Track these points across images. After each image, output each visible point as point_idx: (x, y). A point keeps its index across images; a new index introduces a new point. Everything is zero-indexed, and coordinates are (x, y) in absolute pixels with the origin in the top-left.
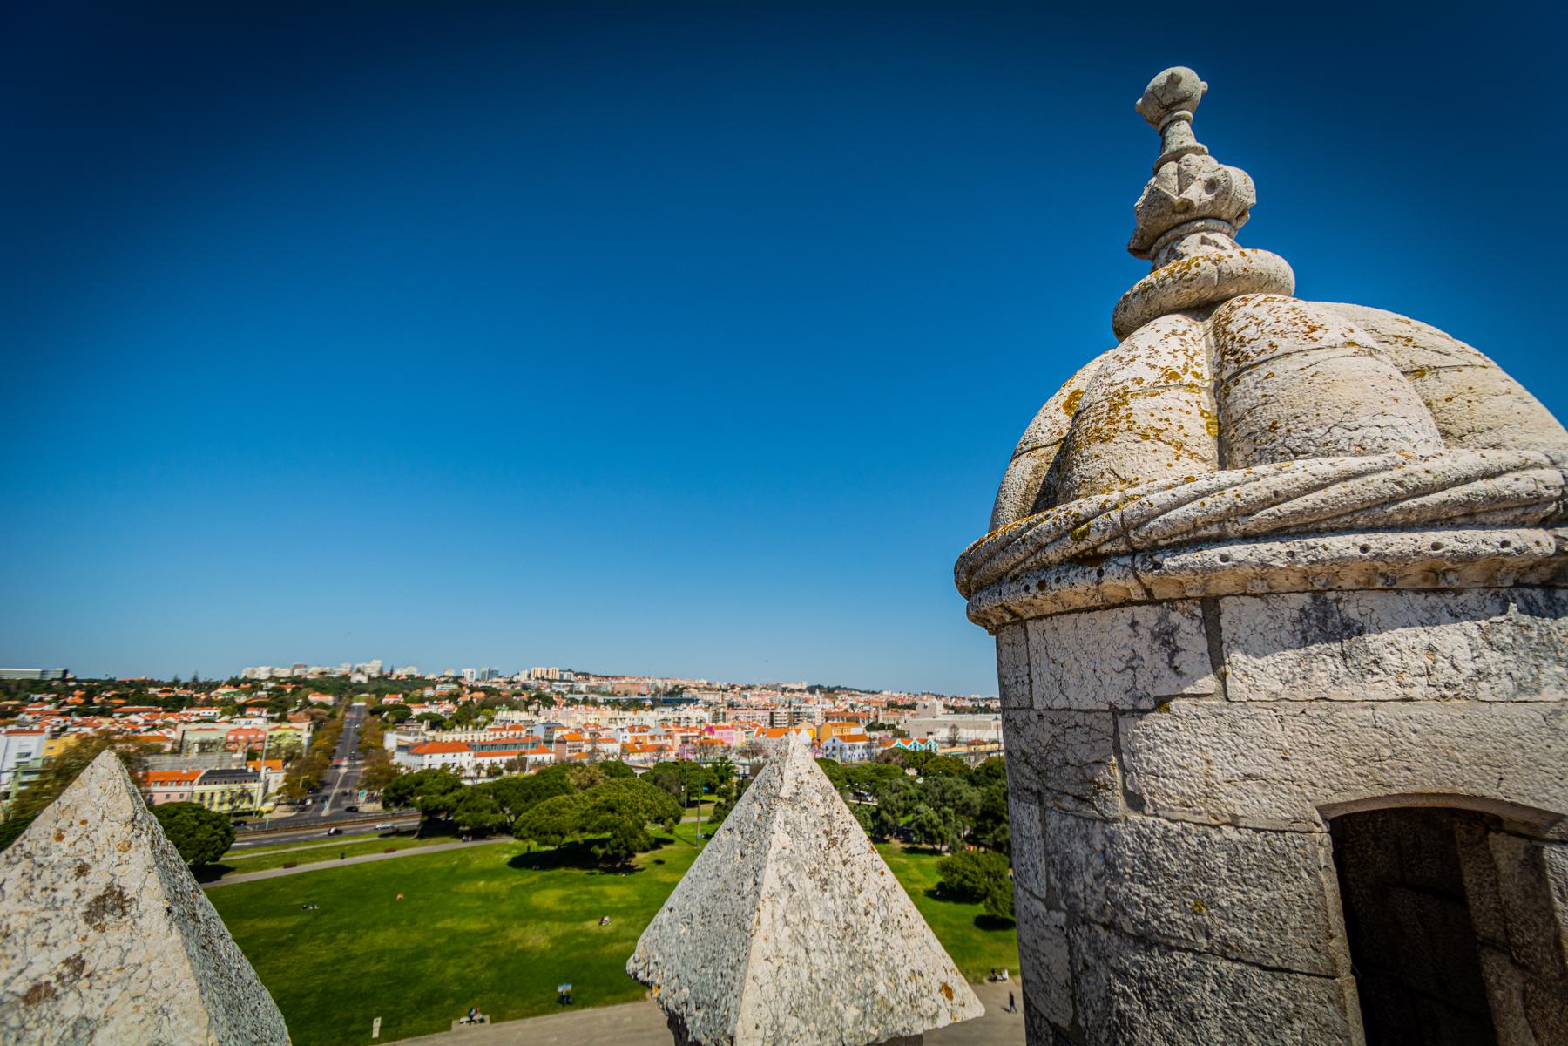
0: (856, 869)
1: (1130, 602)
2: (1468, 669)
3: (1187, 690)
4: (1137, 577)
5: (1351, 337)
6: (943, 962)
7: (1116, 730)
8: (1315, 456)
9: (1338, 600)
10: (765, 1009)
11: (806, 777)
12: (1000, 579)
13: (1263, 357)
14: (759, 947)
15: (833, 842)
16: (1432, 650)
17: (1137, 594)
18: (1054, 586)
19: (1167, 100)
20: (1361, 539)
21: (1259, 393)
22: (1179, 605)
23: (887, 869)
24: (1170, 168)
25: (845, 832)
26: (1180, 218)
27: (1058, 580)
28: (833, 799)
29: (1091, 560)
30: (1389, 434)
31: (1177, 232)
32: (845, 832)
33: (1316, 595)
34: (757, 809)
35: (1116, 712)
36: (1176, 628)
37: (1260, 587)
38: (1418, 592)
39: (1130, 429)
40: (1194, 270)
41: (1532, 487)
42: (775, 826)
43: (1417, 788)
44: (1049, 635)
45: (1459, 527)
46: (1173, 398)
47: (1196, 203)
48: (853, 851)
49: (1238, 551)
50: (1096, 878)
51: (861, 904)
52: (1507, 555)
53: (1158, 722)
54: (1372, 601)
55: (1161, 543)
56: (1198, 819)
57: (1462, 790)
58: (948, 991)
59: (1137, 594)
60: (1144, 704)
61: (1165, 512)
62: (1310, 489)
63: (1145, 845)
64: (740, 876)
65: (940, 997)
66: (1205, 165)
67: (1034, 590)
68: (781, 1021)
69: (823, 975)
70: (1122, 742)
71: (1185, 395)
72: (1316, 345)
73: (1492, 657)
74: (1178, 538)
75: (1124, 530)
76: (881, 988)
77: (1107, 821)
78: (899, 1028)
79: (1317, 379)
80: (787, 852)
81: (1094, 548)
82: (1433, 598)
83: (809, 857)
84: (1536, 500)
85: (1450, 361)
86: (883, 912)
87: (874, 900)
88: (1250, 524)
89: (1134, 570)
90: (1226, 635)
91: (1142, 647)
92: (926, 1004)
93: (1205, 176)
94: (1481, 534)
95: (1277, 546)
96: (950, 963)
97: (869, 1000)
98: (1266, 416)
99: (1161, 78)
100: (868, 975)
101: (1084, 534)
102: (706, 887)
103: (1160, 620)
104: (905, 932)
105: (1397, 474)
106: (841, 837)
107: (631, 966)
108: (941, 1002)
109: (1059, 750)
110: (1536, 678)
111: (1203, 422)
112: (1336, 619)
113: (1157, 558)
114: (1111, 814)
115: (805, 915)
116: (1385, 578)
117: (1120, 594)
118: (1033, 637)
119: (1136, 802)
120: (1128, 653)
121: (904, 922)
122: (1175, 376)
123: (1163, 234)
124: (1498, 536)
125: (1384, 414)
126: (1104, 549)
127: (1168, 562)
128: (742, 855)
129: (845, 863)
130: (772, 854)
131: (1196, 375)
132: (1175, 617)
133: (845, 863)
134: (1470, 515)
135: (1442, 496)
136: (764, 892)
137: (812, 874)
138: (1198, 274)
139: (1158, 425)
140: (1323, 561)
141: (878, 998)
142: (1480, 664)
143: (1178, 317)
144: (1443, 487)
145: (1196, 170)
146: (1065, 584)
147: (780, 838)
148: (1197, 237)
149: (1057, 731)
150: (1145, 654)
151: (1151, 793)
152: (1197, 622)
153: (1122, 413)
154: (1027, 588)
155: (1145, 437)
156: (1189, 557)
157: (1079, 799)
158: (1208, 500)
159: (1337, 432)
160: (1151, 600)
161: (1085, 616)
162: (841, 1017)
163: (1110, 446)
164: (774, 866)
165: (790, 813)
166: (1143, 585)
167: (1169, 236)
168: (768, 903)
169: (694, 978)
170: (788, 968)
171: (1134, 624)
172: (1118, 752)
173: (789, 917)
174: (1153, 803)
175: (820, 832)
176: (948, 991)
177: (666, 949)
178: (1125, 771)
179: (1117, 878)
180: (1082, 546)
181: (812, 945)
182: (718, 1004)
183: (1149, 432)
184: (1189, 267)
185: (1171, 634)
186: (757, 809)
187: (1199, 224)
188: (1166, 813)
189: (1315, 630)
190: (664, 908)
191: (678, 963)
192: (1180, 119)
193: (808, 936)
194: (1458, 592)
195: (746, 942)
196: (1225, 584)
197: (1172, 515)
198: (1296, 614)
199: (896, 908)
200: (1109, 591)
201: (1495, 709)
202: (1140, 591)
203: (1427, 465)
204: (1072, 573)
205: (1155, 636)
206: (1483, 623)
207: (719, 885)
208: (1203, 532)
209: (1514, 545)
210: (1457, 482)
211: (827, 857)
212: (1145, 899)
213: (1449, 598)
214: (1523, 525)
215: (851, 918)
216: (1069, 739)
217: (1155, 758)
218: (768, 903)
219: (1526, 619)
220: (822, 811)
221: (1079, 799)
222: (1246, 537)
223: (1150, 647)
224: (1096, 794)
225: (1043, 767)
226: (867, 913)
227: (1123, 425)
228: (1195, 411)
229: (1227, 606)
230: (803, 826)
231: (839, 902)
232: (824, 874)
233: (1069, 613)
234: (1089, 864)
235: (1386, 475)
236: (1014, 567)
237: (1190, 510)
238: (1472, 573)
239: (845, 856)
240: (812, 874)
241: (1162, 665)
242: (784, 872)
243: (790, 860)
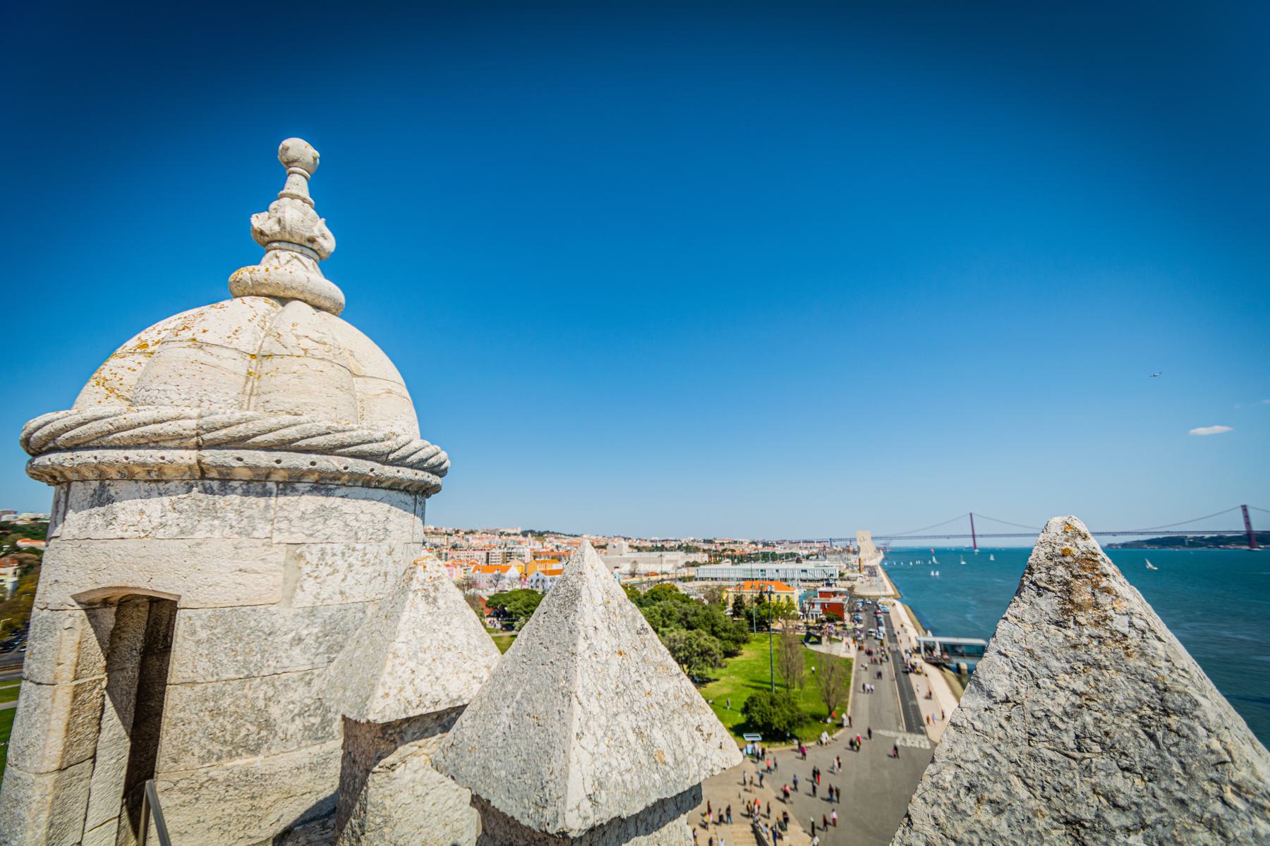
2: (156, 521)
16: (142, 512)
20: (96, 453)
54: (123, 486)
57: (130, 585)
82: (153, 485)
110: (194, 527)
116: (128, 474)
135: (131, 432)
142: (163, 520)
145: (294, 209)
155: (98, 384)
187: (275, 245)
194: (167, 482)
206: (174, 498)
210: (139, 425)
213: (161, 485)
219: (202, 496)
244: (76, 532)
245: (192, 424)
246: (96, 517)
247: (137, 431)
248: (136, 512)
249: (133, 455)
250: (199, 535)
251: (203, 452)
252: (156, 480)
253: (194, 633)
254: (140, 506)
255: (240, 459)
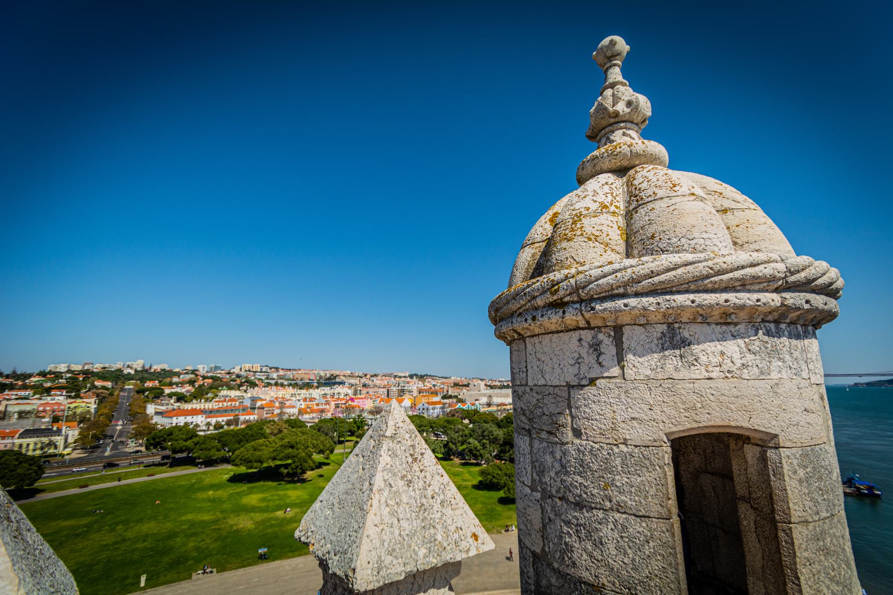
0: (428, 474)
1: (578, 328)
2: (739, 363)
3: (605, 375)
4: (582, 315)
5: (693, 191)
6: (473, 521)
7: (569, 396)
8: (672, 252)
9: (679, 328)
10: (374, 553)
11: (401, 425)
12: (512, 315)
13: (650, 199)
14: (371, 519)
15: (415, 460)
16: (722, 354)
17: (582, 324)
18: (540, 319)
19: (609, 54)
20: (692, 296)
21: (647, 218)
22: (603, 330)
23: (444, 473)
24: (609, 92)
25: (422, 454)
26: (613, 120)
27: (542, 316)
28: (416, 436)
29: (559, 305)
30: (708, 242)
31: (610, 128)
32: (422, 454)
33: (669, 325)
34: (372, 443)
35: (570, 387)
36: (601, 342)
37: (642, 321)
38: (717, 324)
39: (582, 235)
40: (618, 150)
41: (772, 272)
42: (382, 452)
43: (712, 423)
44: (537, 345)
45: (738, 291)
46: (605, 219)
47: (621, 113)
48: (426, 464)
49: (633, 302)
50: (556, 474)
51: (429, 492)
52: (759, 306)
53: (590, 391)
54: (696, 328)
55: (595, 296)
56: (608, 441)
57: (733, 424)
58: (475, 537)
59: (582, 324)
60: (584, 382)
61: (597, 280)
62: (669, 270)
63: (581, 456)
64: (361, 480)
65: (471, 540)
66: (626, 92)
67: (530, 321)
68: (383, 558)
69: (407, 532)
70: (572, 402)
71: (611, 218)
72: (675, 194)
73: (750, 357)
74: (604, 294)
75: (576, 289)
76: (439, 537)
77: (563, 444)
78: (448, 558)
79: (675, 212)
80: (389, 466)
81: (561, 299)
82: (724, 327)
83: (401, 469)
84: (773, 279)
85: (739, 206)
86: (442, 497)
87: (437, 491)
88: (639, 287)
89: (581, 311)
90: (625, 346)
91: (584, 352)
92: (464, 545)
93: (626, 99)
94: (748, 295)
95: (651, 299)
96: (477, 522)
97: (432, 544)
98: (650, 230)
99: (606, 41)
100: (432, 531)
101: (557, 291)
102: (342, 488)
103: (593, 338)
104: (453, 507)
105: (710, 263)
106: (420, 457)
107: (297, 534)
108: (471, 543)
109: (540, 407)
110: (769, 368)
111: (619, 233)
112: (678, 338)
113: (593, 305)
114: (565, 440)
115: (398, 500)
116: (702, 317)
117: (574, 323)
118: (529, 347)
119: (577, 433)
120: (576, 355)
121: (453, 501)
122: (606, 207)
123: (604, 129)
124: (755, 296)
125: (706, 232)
126: (567, 299)
127: (598, 307)
128: (363, 469)
129: (421, 471)
130: (380, 467)
131: (617, 207)
132: (601, 336)
133: (421, 471)
134: (743, 285)
135: (730, 275)
136: (375, 488)
137: (402, 478)
138: (620, 152)
139: (597, 233)
140: (673, 308)
141: (437, 542)
142: (744, 361)
143: (610, 175)
144: (731, 271)
145: (623, 95)
146: (546, 318)
147: (385, 459)
148: (621, 131)
149: (540, 397)
150: (585, 355)
151: (585, 429)
152: (611, 339)
153: (579, 226)
154: (526, 320)
155: (590, 239)
156: (608, 305)
157: (550, 433)
158: (619, 274)
159: (683, 240)
160: (589, 327)
161: (556, 335)
162: (416, 554)
163: (572, 243)
164: (381, 474)
165: (391, 444)
166: (585, 319)
167: (607, 130)
168: (377, 496)
169: (333, 538)
170: (387, 530)
171: (580, 340)
172: (570, 408)
173: (389, 502)
174: (586, 434)
175: (408, 455)
176: (475, 537)
177: (318, 523)
178: (573, 417)
179: (567, 473)
180: (555, 297)
181: (401, 516)
182: (345, 553)
183: (592, 237)
184: (616, 148)
185: (598, 345)
186: (372, 443)
187: (622, 125)
188: (592, 439)
189: (668, 343)
190: (318, 501)
191: (324, 531)
192: (615, 65)
193: (399, 511)
194: (736, 324)
195: (364, 517)
196: (625, 319)
197: (600, 282)
198: (659, 335)
199: (449, 494)
200: (568, 322)
201: (751, 383)
202: (584, 322)
203: (724, 259)
204: (550, 312)
205: (591, 346)
206: (747, 340)
207: (350, 486)
208: (616, 292)
209: (762, 301)
211: (411, 468)
212: (580, 484)
213: (732, 328)
214: (767, 291)
215: (424, 501)
216: (545, 401)
217: (588, 410)
218: (377, 496)
219: (766, 338)
220: (409, 443)
221: (550, 433)
222: (637, 295)
223: (588, 352)
224: (558, 430)
225: (532, 416)
226: (433, 498)
227: (579, 232)
228: (615, 226)
229: (627, 330)
230: (399, 452)
231: (417, 492)
232: (410, 477)
233: (548, 333)
234: (553, 467)
235: (705, 264)
236: (520, 308)
237: (610, 279)
238: (743, 315)
239: (422, 467)
240: (402, 478)
241: (593, 361)
242: (386, 477)
243: (390, 471)
244: (648, 372)
245: (781, 267)
246: (672, 361)
247: (738, 274)
248: (718, 354)
249: (733, 298)
250: (774, 375)
251: (784, 295)
252: (727, 322)
253: (795, 472)
254: (720, 348)
255: (807, 302)
